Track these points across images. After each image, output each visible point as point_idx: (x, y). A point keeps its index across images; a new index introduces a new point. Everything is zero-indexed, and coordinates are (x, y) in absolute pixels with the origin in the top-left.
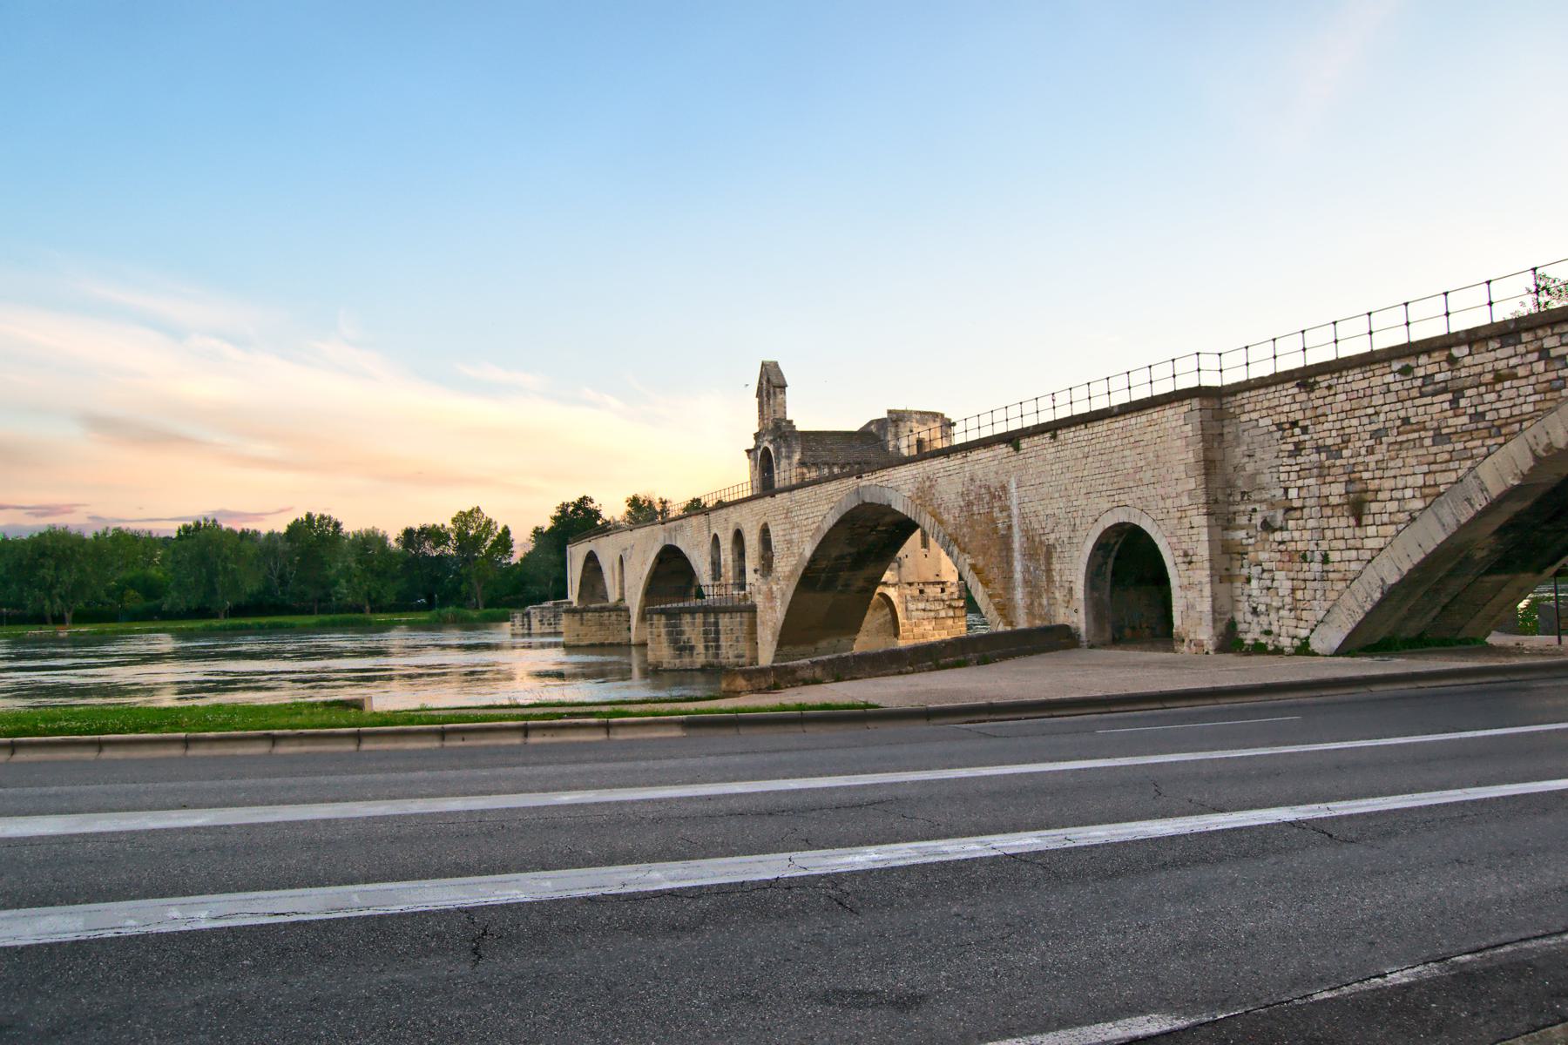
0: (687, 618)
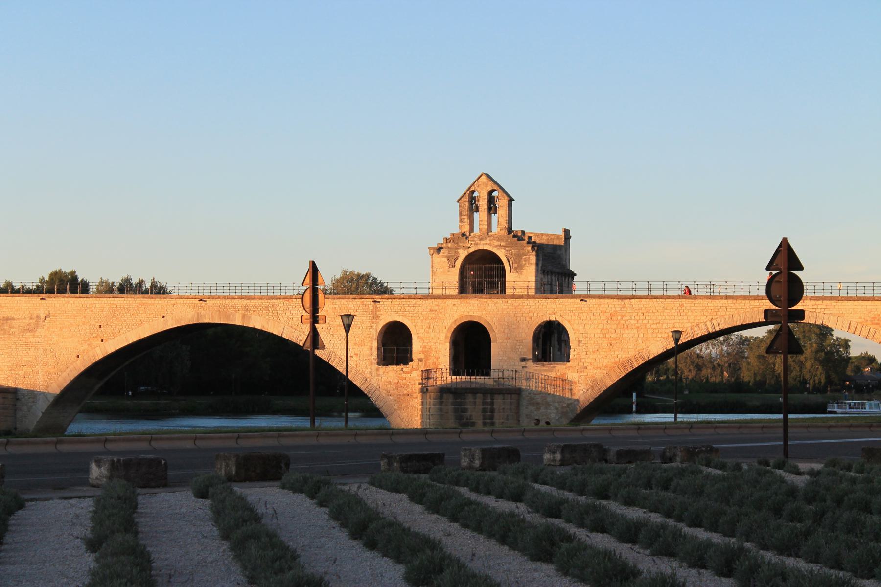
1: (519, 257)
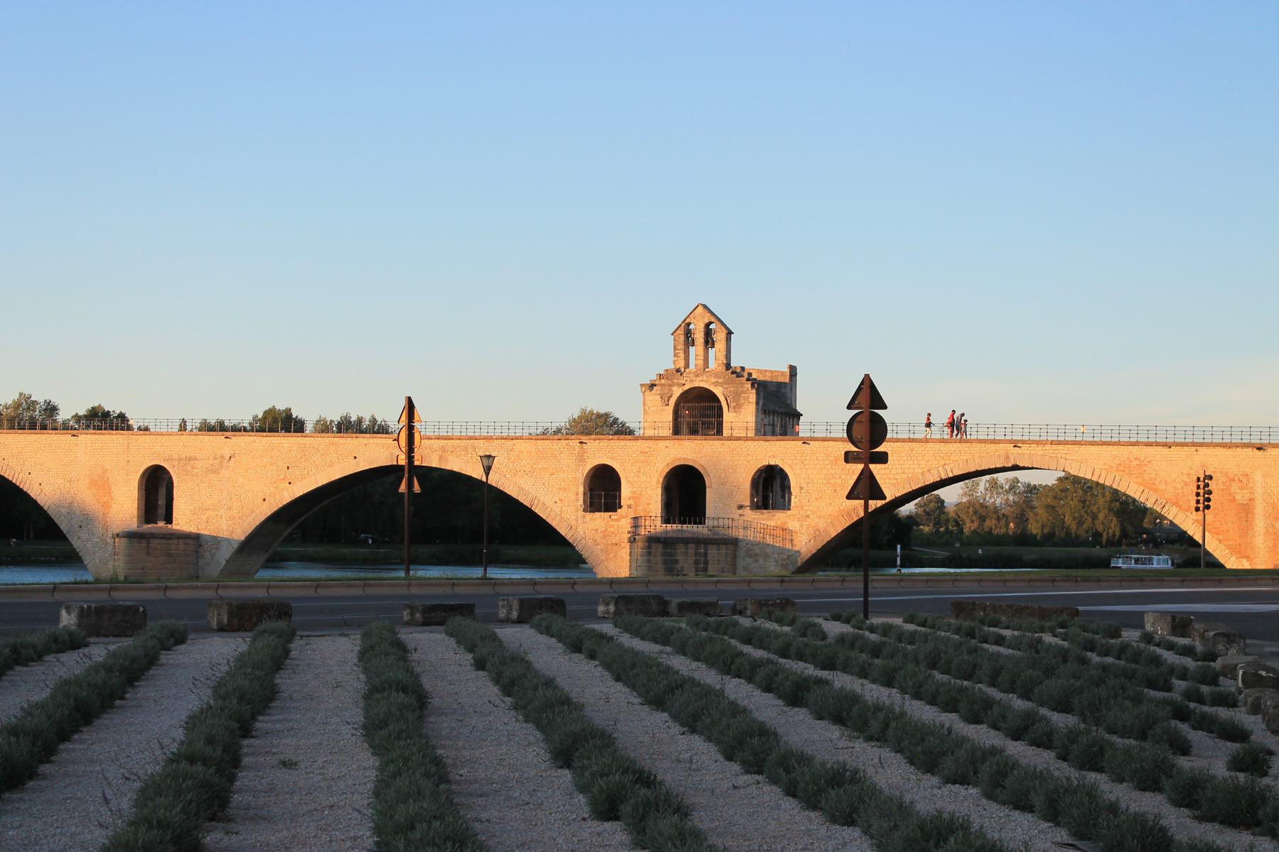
0: (681, 545)
1: (737, 395)
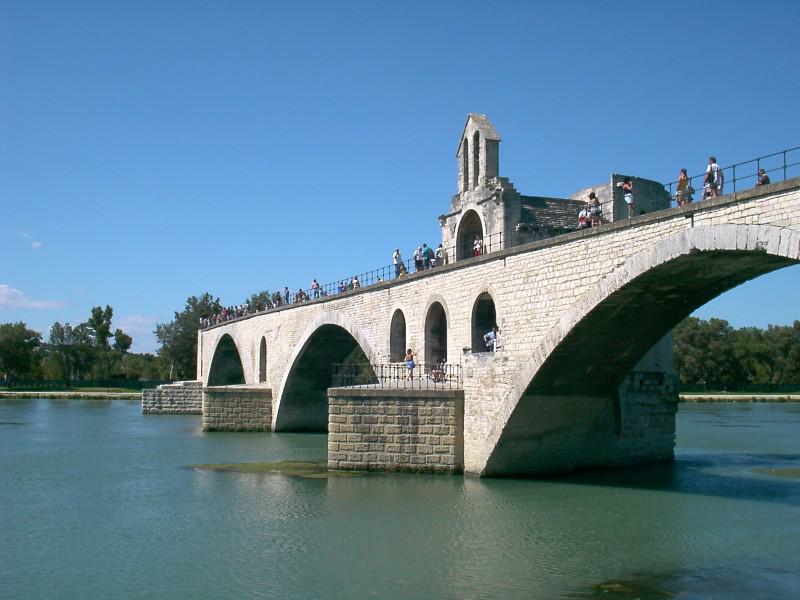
1: (490, 213)
